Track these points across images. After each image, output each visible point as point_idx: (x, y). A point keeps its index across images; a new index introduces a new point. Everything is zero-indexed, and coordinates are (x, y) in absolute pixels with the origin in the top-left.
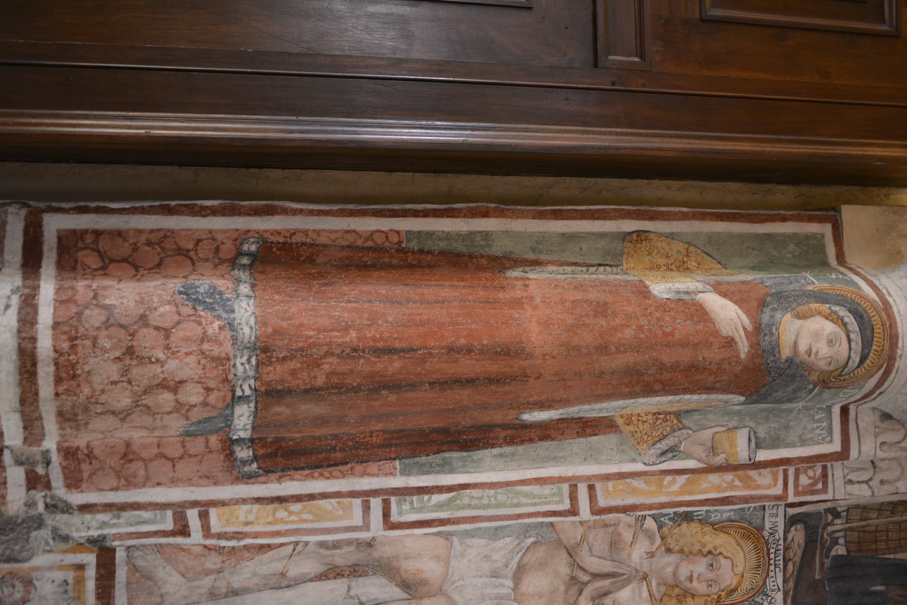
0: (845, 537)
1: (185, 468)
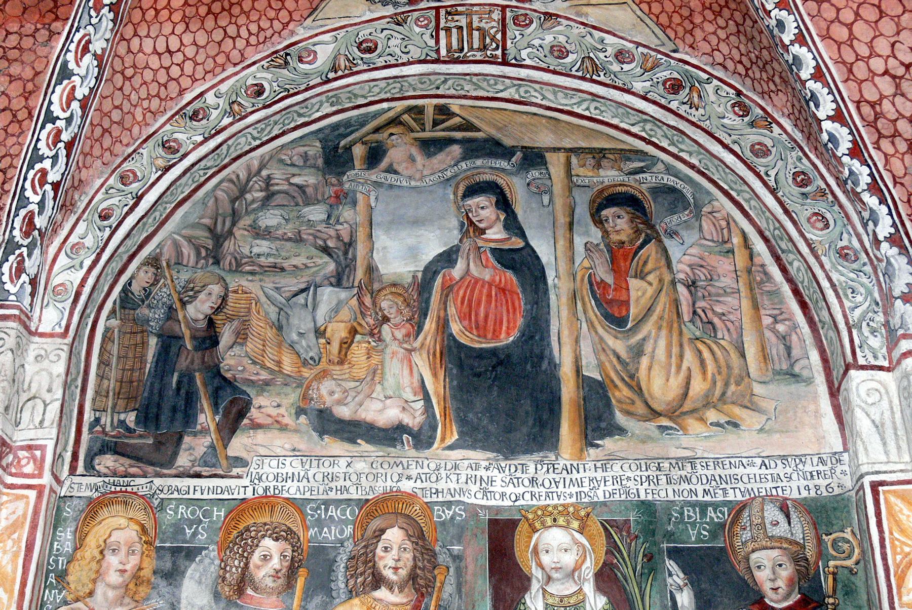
0: (119, 413)
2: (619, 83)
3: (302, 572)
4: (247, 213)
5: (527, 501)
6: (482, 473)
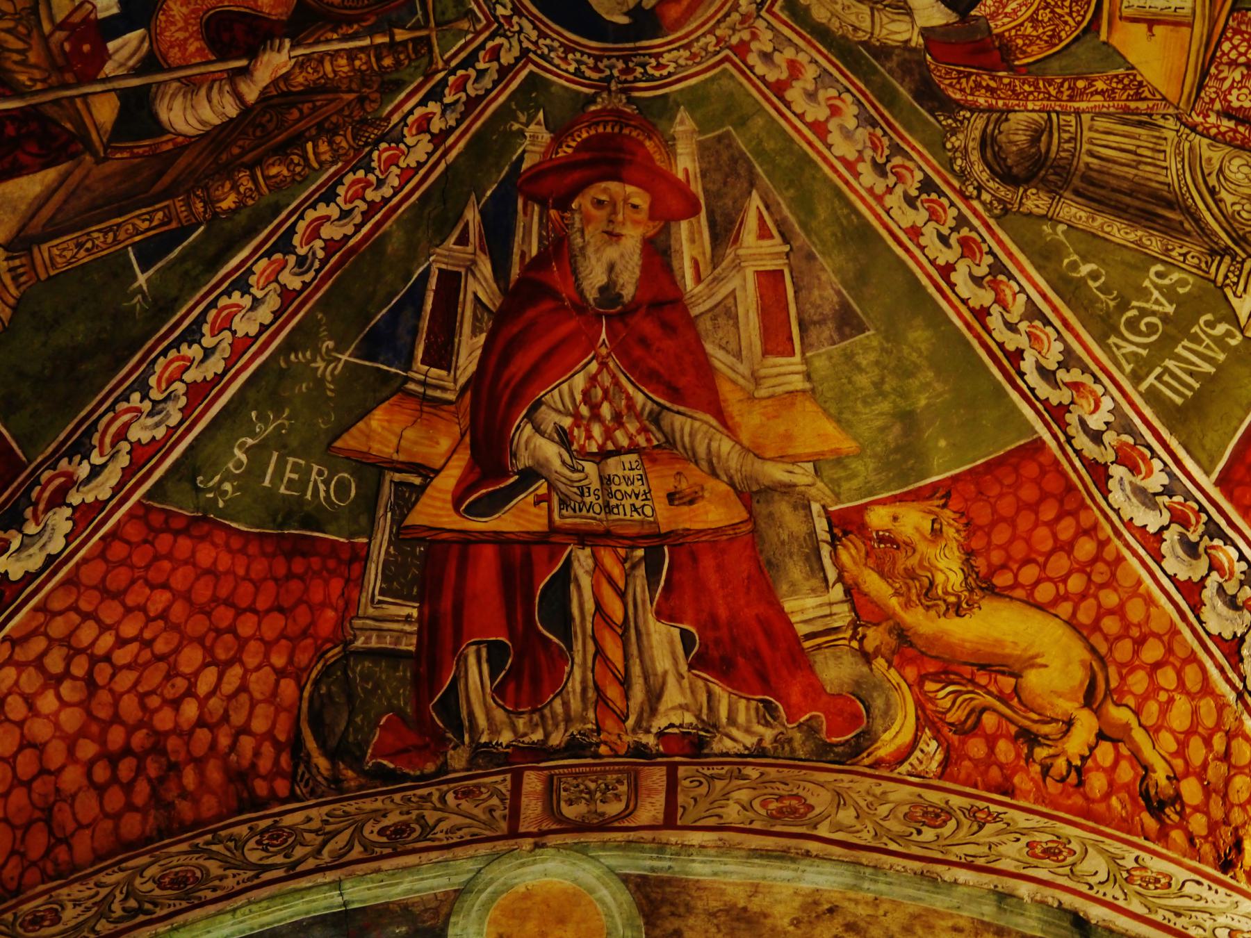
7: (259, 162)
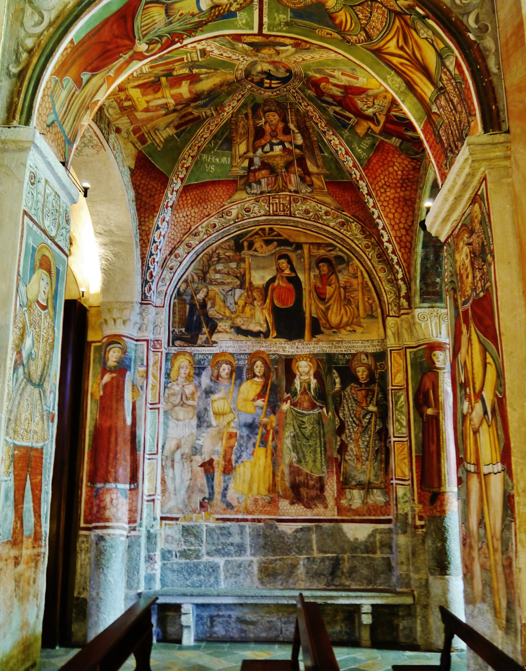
1: (134, 499)
2: (325, 223)
3: (234, 373)
4: (213, 265)
5: (295, 353)
6: (283, 345)
7: (309, 133)
